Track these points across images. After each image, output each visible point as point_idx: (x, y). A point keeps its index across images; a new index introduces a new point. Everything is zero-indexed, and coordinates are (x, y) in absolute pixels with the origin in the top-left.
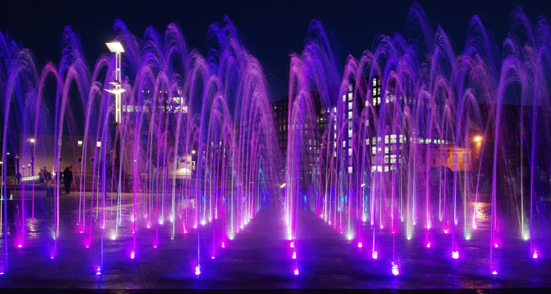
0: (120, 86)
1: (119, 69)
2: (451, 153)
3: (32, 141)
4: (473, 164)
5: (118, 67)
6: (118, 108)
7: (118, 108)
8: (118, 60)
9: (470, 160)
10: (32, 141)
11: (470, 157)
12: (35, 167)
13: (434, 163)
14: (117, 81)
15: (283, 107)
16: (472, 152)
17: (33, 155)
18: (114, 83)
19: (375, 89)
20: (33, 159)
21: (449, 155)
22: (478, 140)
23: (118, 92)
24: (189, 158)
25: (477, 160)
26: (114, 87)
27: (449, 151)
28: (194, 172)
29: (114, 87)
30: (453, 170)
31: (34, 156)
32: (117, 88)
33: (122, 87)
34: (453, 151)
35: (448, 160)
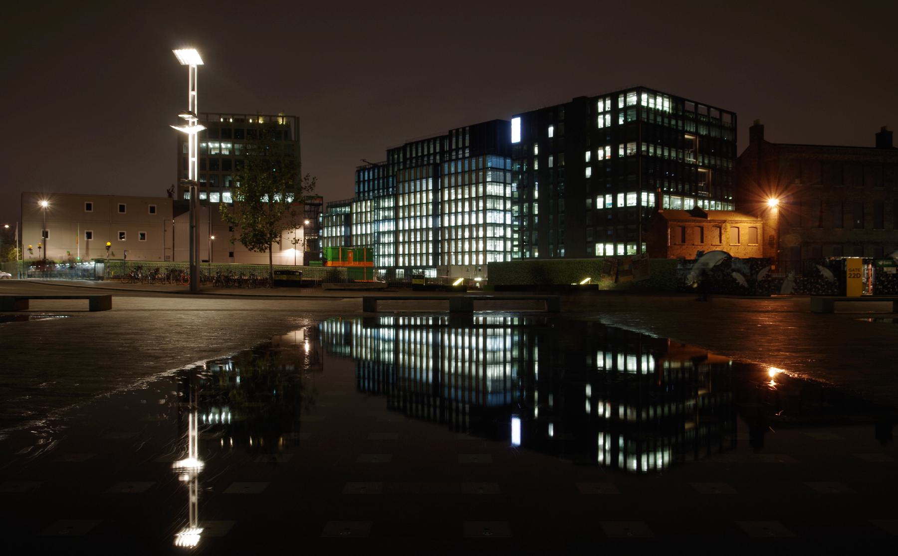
0: (196, 120)
1: (195, 93)
2: (728, 225)
4: (764, 245)
5: (193, 90)
8: (193, 79)
9: (760, 238)
11: (760, 231)
12: (48, 247)
13: (702, 241)
14: (192, 113)
16: (764, 224)
17: (44, 227)
19: (607, 109)
20: (45, 235)
22: (773, 204)
24: (300, 233)
25: (772, 237)
26: (187, 122)
27: (725, 221)
28: (306, 254)
29: (187, 122)
30: (732, 255)
31: (48, 230)
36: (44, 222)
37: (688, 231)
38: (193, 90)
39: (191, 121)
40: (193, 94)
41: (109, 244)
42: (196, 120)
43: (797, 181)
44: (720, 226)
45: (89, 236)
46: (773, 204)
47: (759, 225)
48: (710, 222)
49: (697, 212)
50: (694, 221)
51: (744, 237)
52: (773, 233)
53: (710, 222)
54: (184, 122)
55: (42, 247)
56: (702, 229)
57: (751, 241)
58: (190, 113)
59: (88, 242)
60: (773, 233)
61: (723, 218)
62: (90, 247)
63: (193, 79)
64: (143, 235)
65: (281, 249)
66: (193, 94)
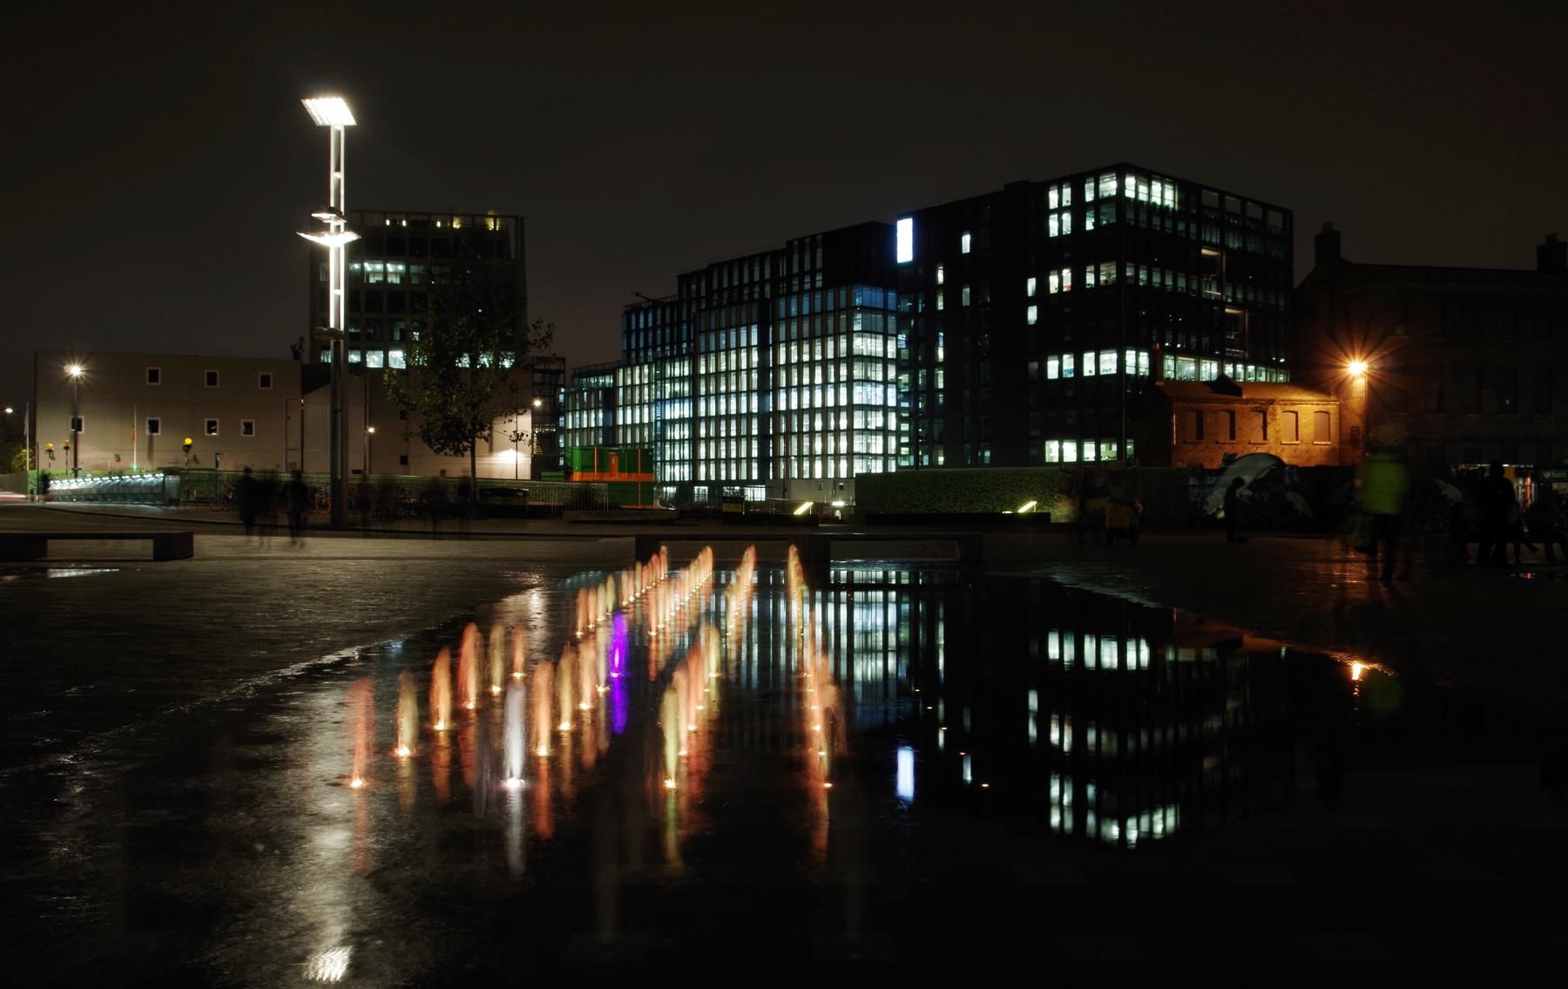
0: (342, 223)
3: (75, 370)
4: (1341, 443)
5: (338, 169)
6: (338, 287)
7: (338, 287)
8: (337, 150)
9: (1334, 430)
10: (75, 370)
12: (81, 446)
13: (1233, 437)
14: (335, 210)
15: (790, 267)
16: (1340, 407)
17: (75, 413)
18: (324, 216)
20: (77, 425)
21: (1274, 414)
22: (1357, 370)
23: (335, 240)
24: (524, 423)
25: (1354, 430)
26: (326, 227)
27: (1272, 402)
29: (326, 227)
31: (82, 417)
32: (332, 228)
33: (349, 227)
34: (1285, 402)
35: (1270, 430)
36: (74, 401)
37: (1209, 419)
38: (338, 169)
39: (333, 224)
40: (337, 177)
41: (188, 441)
42: (342, 223)
43: (1399, 331)
44: (1264, 410)
45: (154, 427)
46: (1357, 370)
47: (1332, 408)
48: (1246, 402)
49: (1224, 385)
50: (1218, 401)
51: (1307, 430)
52: (1357, 421)
53: (1246, 402)
54: (321, 227)
55: (71, 446)
56: (1232, 414)
57: (1318, 436)
58: (331, 210)
59: (151, 438)
60: (1357, 421)
61: (1270, 396)
62: (155, 447)
63: (337, 150)
64: (249, 427)
65: (491, 450)
66: (337, 177)
